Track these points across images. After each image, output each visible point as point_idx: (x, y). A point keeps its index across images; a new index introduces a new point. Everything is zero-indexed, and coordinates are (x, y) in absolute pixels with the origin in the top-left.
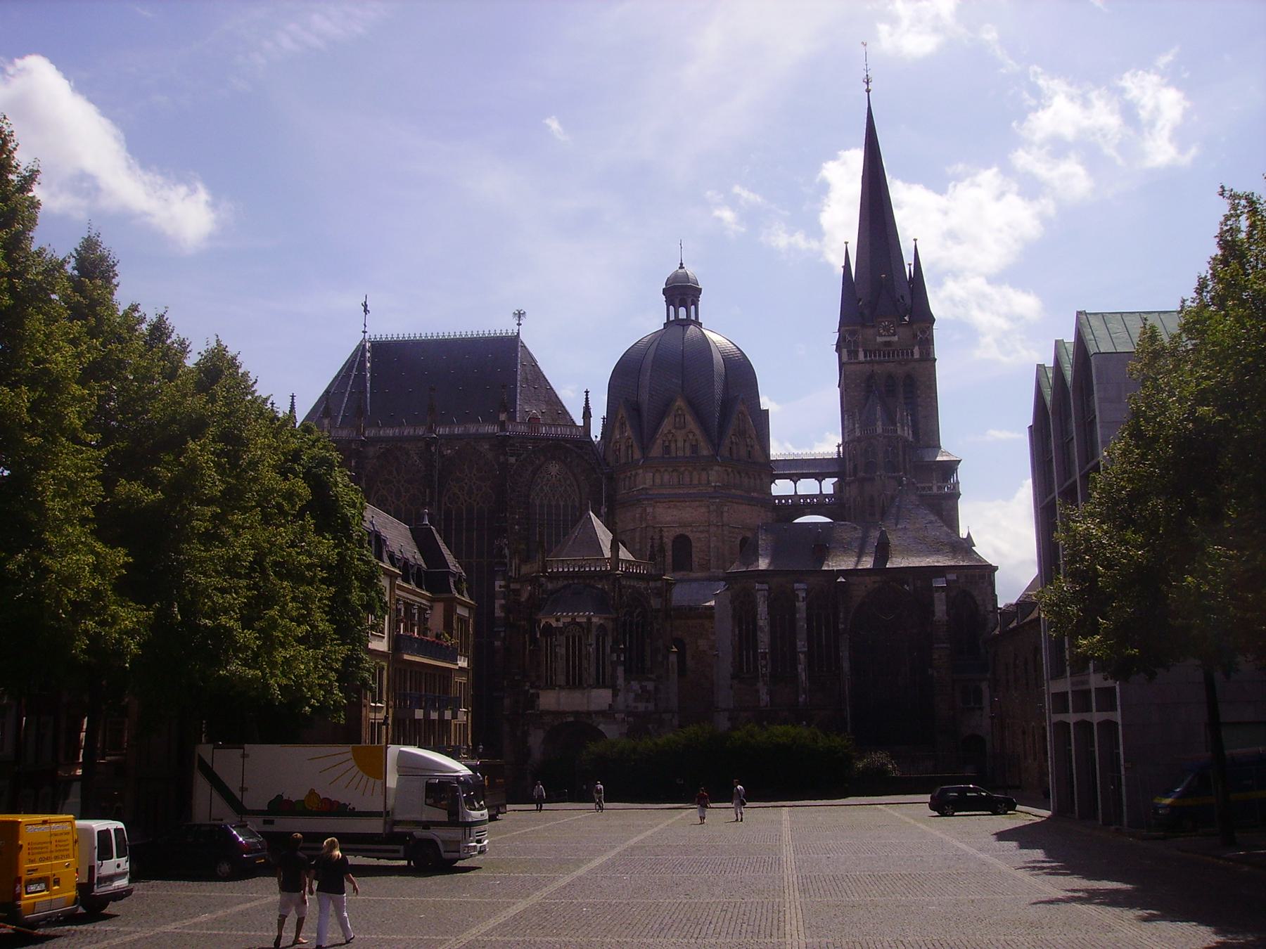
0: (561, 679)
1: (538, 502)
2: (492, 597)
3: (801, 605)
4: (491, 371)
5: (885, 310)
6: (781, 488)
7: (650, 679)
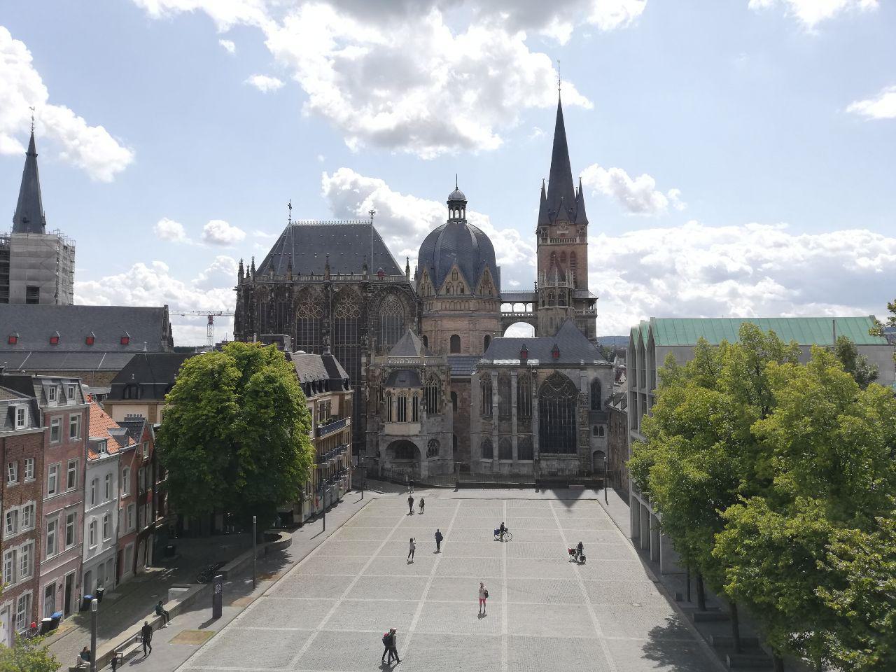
0: (395, 418)
1: (383, 315)
2: (360, 364)
3: (514, 383)
4: (358, 242)
5: (562, 211)
6: (506, 308)
7: (439, 416)
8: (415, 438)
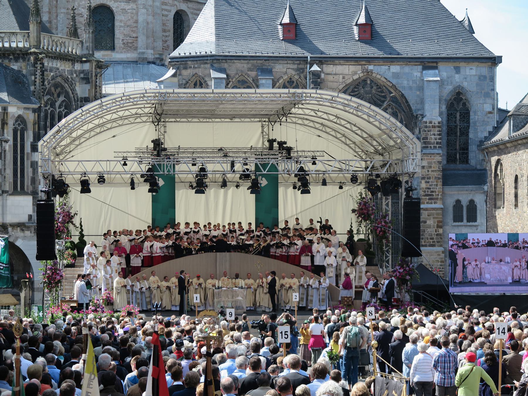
8: (18, 232)
